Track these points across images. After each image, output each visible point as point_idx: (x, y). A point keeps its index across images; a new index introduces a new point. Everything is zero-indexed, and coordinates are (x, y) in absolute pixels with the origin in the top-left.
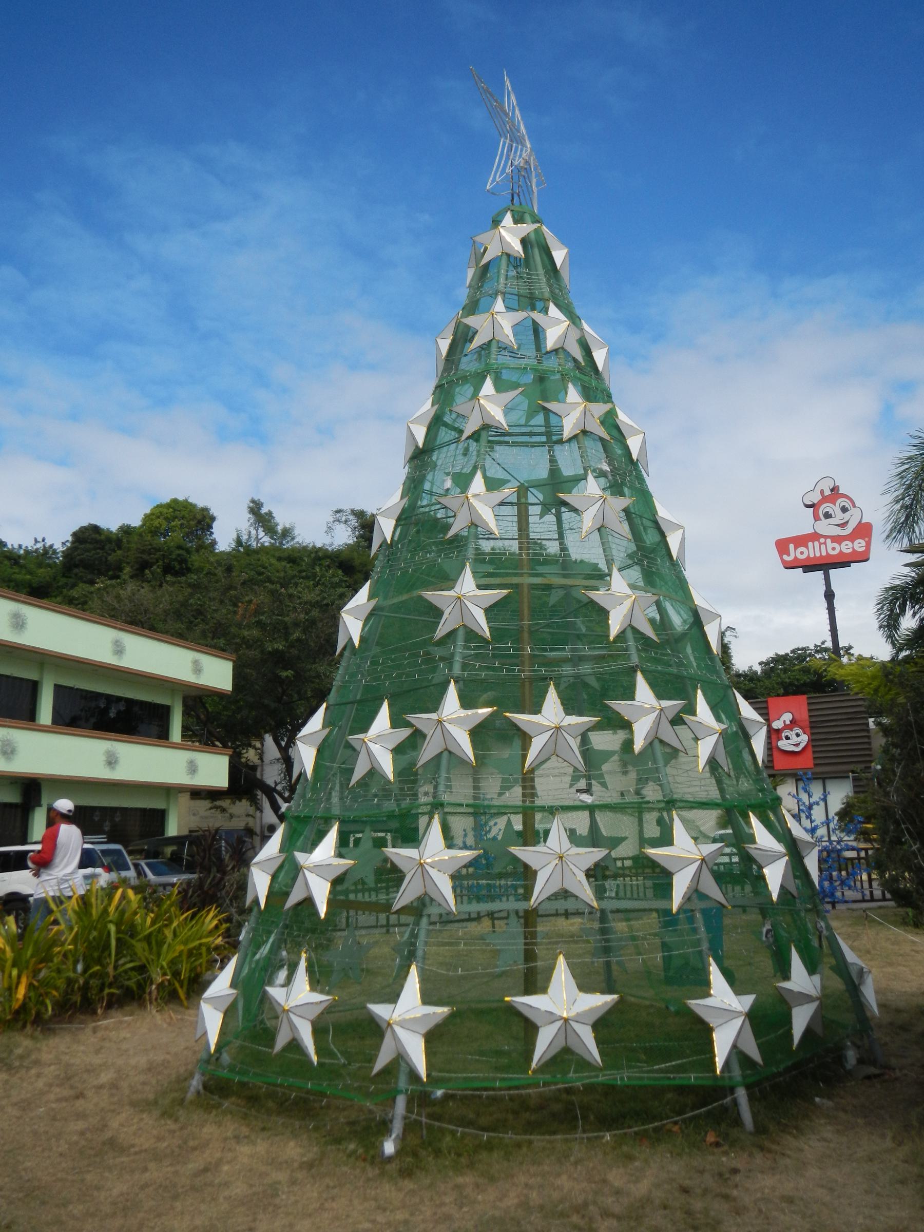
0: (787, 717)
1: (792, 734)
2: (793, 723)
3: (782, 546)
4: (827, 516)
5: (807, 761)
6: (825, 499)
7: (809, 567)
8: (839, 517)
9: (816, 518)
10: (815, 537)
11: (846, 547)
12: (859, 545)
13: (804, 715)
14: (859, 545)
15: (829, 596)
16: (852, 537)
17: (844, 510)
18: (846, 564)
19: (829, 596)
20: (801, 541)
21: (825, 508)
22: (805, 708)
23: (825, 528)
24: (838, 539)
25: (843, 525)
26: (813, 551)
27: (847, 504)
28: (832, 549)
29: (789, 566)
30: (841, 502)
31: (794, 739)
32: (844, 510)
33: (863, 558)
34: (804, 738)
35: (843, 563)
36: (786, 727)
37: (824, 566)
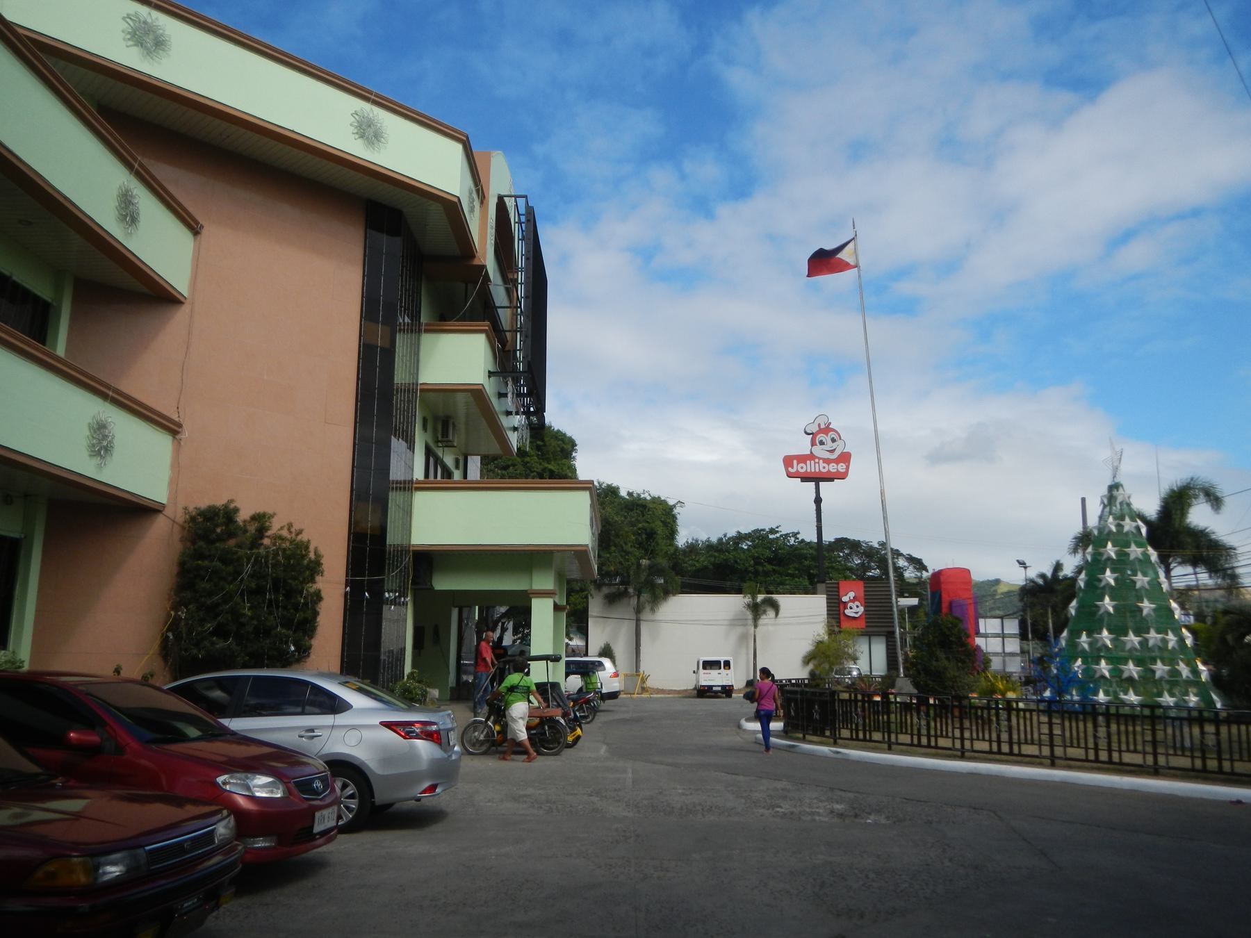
0: (852, 595)
1: (853, 605)
2: (855, 599)
3: (788, 461)
4: (822, 443)
5: (862, 624)
6: (821, 431)
7: (805, 478)
8: (829, 445)
9: (813, 444)
10: (812, 457)
11: (833, 468)
12: (841, 467)
13: (862, 594)
14: (841, 467)
15: (818, 501)
16: (837, 461)
17: (833, 440)
18: (831, 480)
19: (818, 501)
20: (802, 459)
21: (821, 437)
22: (862, 590)
23: (819, 451)
24: (827, 461)
25: (832, 451)
26: (810, 467)
27: (836, 437)
28: (823, 468)
29: (790, 475)
30: (832, 434)
31: (855, 609)
32: (833, 440)
33: (842, 476)
34: (861, 609)
35: (830, 478)
36: (850, 601)
37: (817, 479)
